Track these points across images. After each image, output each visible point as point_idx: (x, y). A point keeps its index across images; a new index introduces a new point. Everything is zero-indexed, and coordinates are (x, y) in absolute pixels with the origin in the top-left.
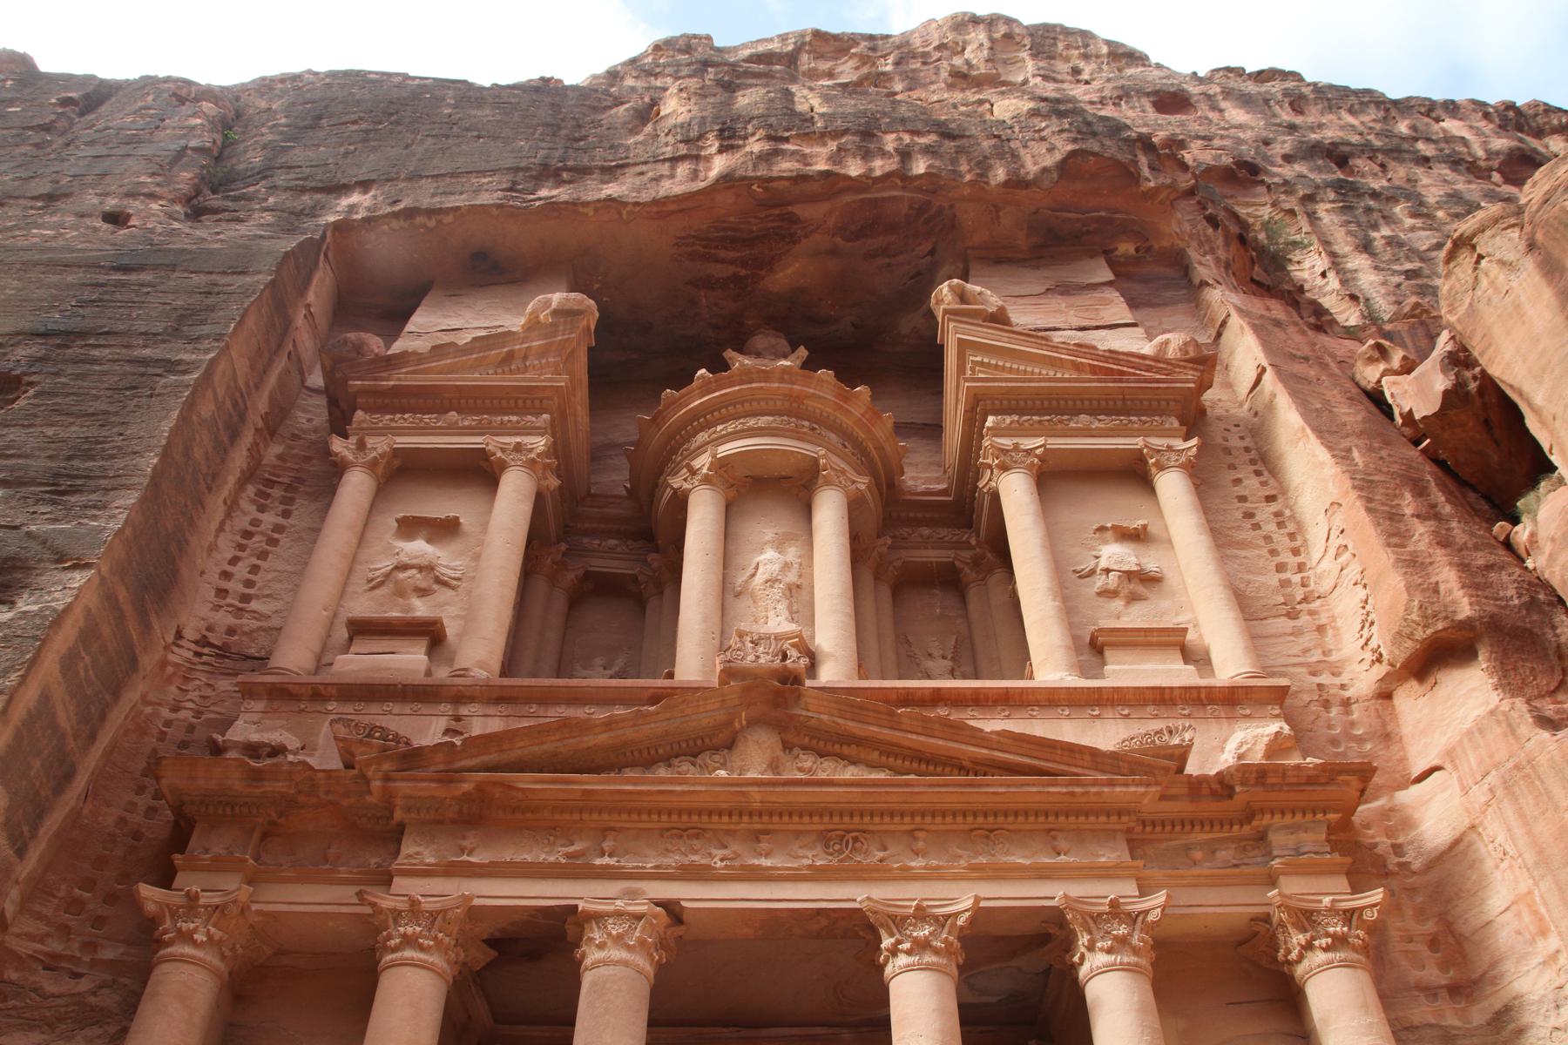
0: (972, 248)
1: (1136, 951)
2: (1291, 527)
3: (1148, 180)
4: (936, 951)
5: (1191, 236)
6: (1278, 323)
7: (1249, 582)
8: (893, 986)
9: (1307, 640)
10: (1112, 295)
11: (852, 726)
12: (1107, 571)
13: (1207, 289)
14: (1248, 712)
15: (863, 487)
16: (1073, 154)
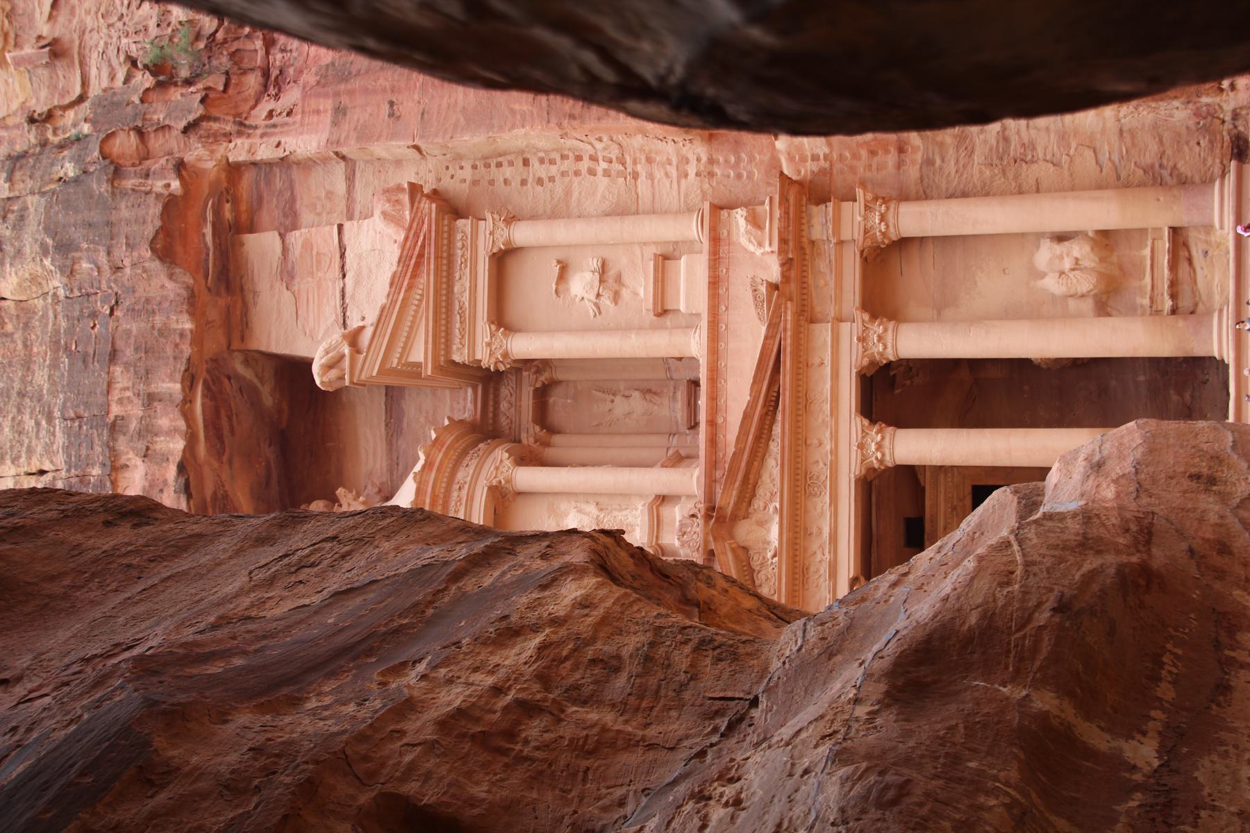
0: (229, 345)
1: (886, 330)
2: (556, 156)
3: (168, 185)
4: (883, 438)
5: (212, 152)
6: (340, 112)
7: (604, 197)
8: (898, 463)
9: (659, 174)
10: (296, 238)
11: (740, 477)
12: (598, 295)
13: (292, 157)
14: (725, 232)
15: (506, 455)
16: (153, 250)
